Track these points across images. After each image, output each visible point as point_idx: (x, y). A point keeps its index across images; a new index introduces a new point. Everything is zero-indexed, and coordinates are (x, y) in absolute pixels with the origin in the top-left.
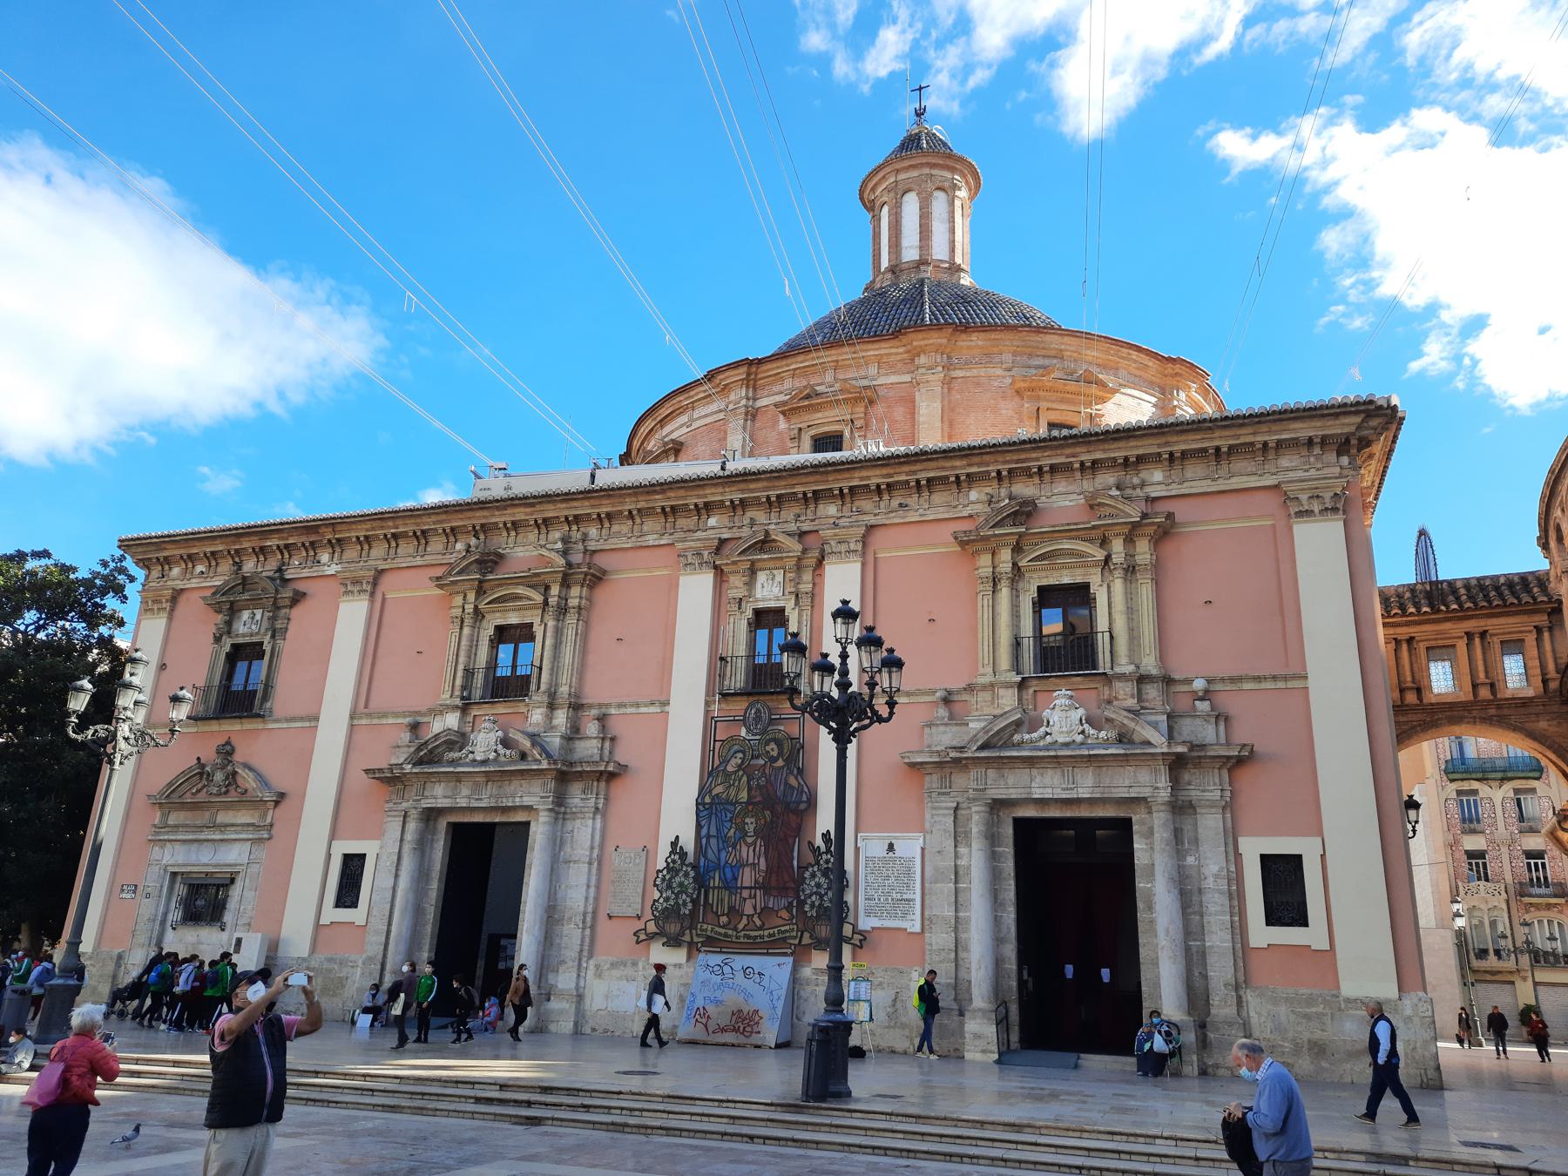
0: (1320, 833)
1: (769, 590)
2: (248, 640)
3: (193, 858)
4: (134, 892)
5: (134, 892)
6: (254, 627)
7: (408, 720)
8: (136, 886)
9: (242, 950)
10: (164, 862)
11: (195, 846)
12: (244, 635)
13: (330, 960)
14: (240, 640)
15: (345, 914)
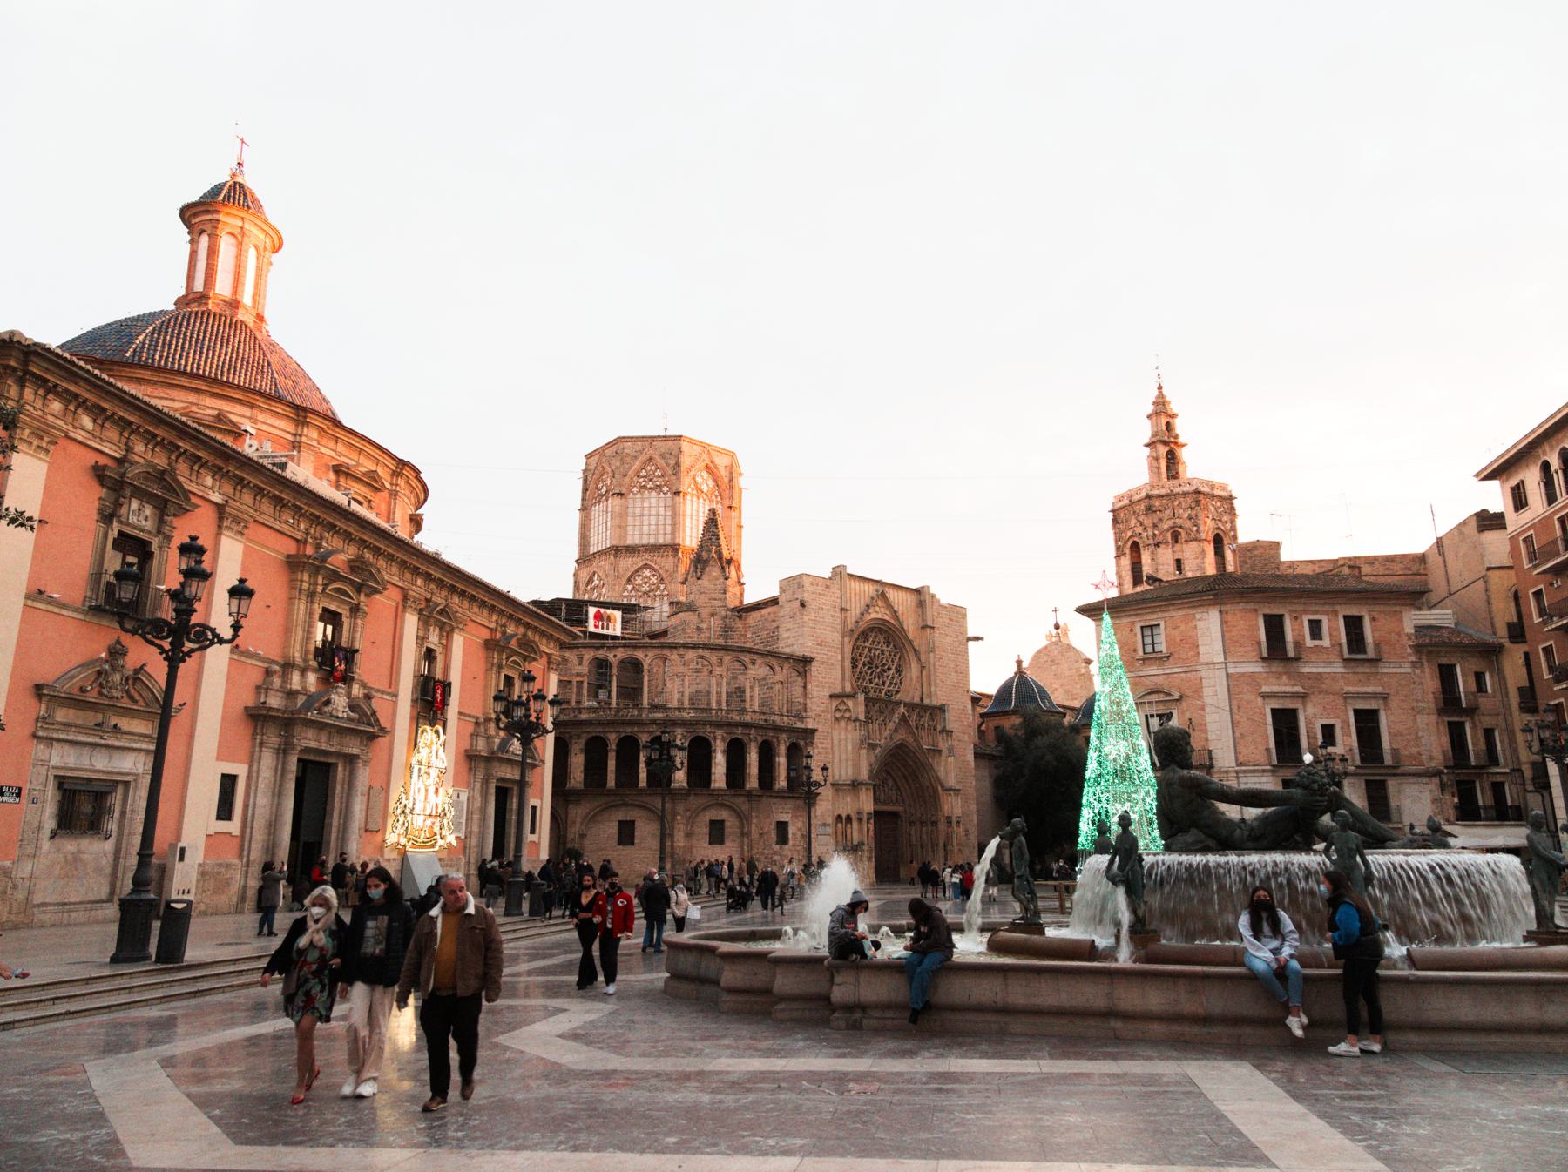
0: (542, 799)
1: (434, 639)
2: (135, 533)
3: (85, 763)
4: (18, 795)
5: (18, 795)
6: (143, 522)
7: (266, 665)
8: (20, 789)
9: (186, 858)
10: (52, 763)
11: (86, 751)
12: (135, 527)
13: (220, 865)
14: (129, 530)
15: (224, 826)
